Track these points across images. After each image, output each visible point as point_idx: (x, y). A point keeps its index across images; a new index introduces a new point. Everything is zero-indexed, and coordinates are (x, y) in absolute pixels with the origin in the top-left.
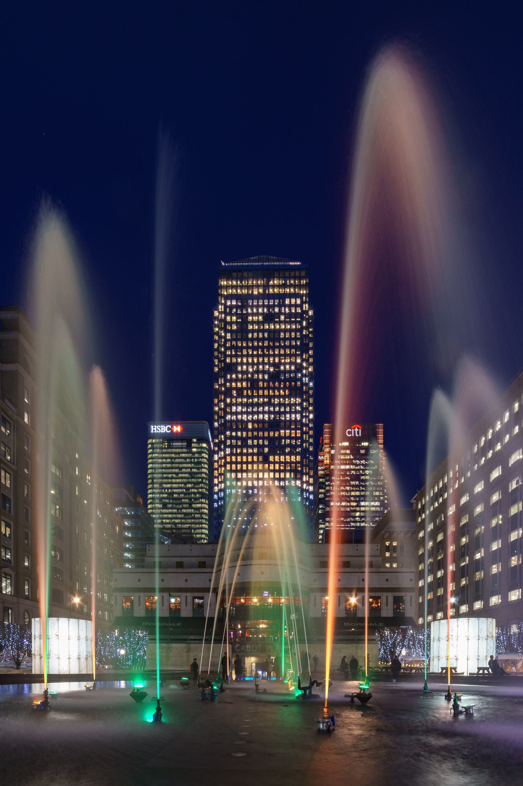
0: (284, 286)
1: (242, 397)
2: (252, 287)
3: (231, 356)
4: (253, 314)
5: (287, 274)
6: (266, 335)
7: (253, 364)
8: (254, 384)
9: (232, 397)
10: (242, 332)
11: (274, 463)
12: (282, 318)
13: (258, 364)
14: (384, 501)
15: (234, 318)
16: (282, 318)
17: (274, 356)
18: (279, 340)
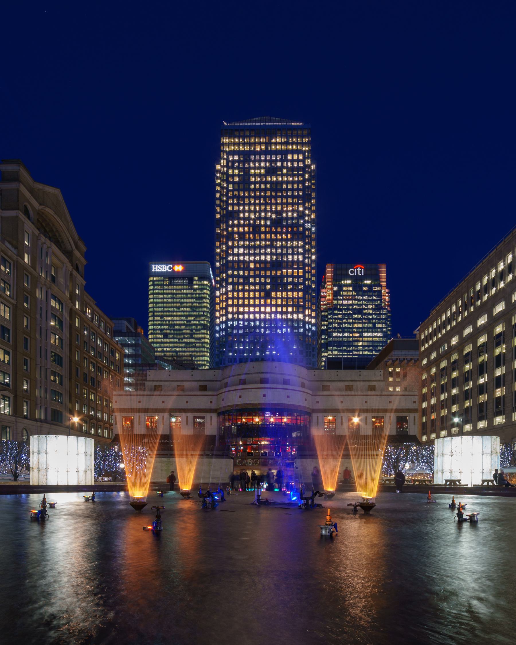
0: (287, 143)
1: (244, 240)
2: (255, 144)
3: (233, 204)
4: (255, 168)
5: (289, 133)
6: (268, 186)
7: (255, 211)
8: (256, 229)
9: (233, 240)
10: (245, 182)
11: (276, 298)
12: (285, 171)
13: (260, 211)
14: (387, 332)
15: (236, 172)
16: (285, 171)
17: (276, 204)
18: (281, 190)
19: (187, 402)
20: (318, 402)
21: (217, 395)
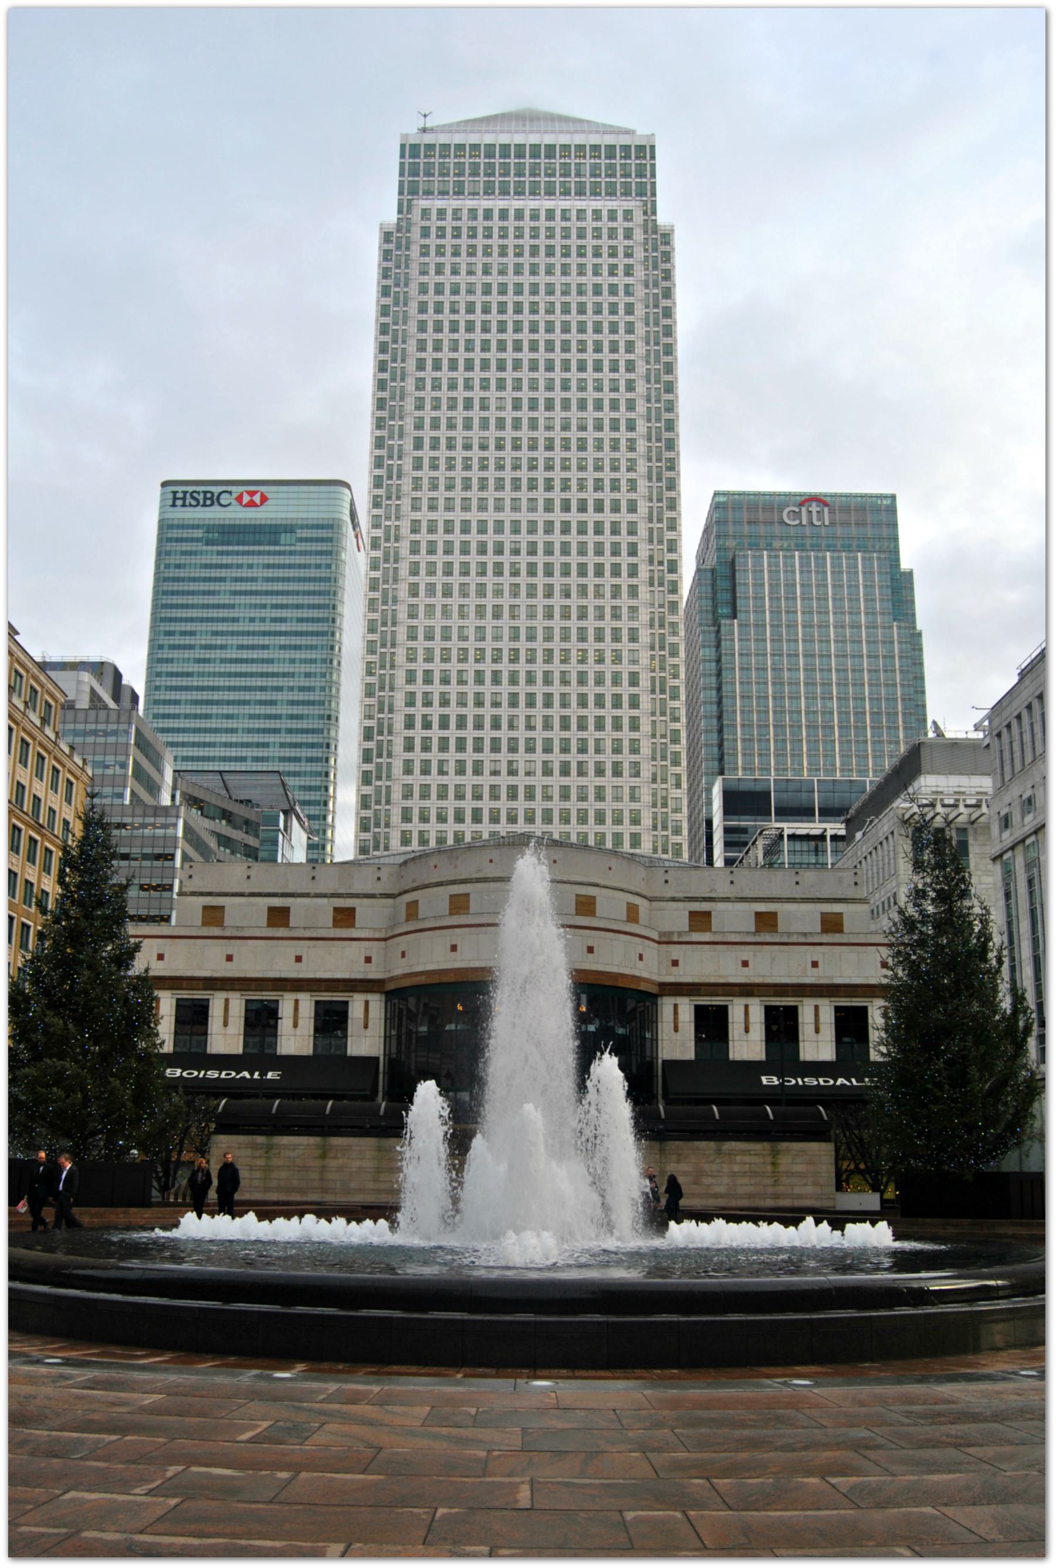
19: (299, 959)
20: (675, 963)
21: (385, 940)
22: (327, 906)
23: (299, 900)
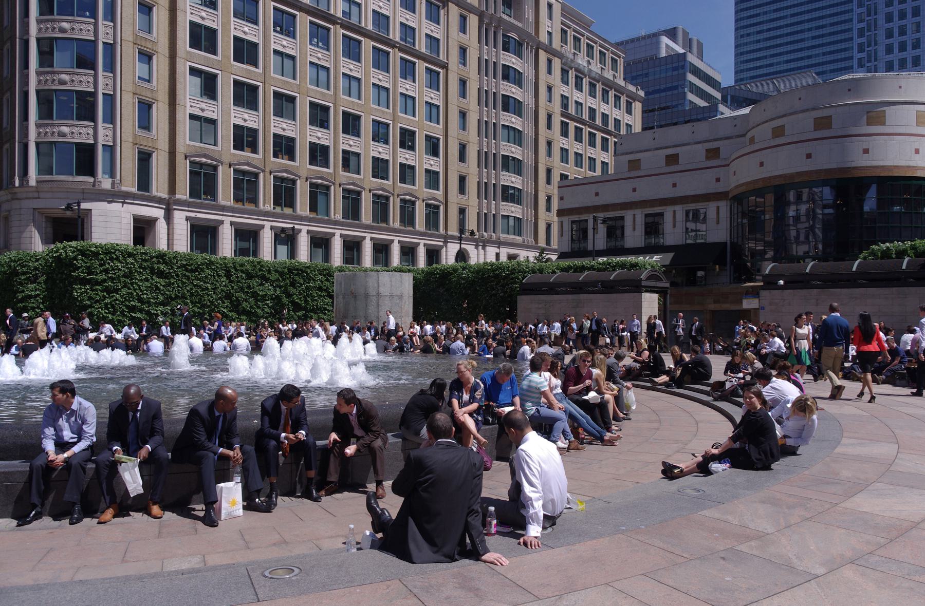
22: (701, 149)
23: (684, 148)
